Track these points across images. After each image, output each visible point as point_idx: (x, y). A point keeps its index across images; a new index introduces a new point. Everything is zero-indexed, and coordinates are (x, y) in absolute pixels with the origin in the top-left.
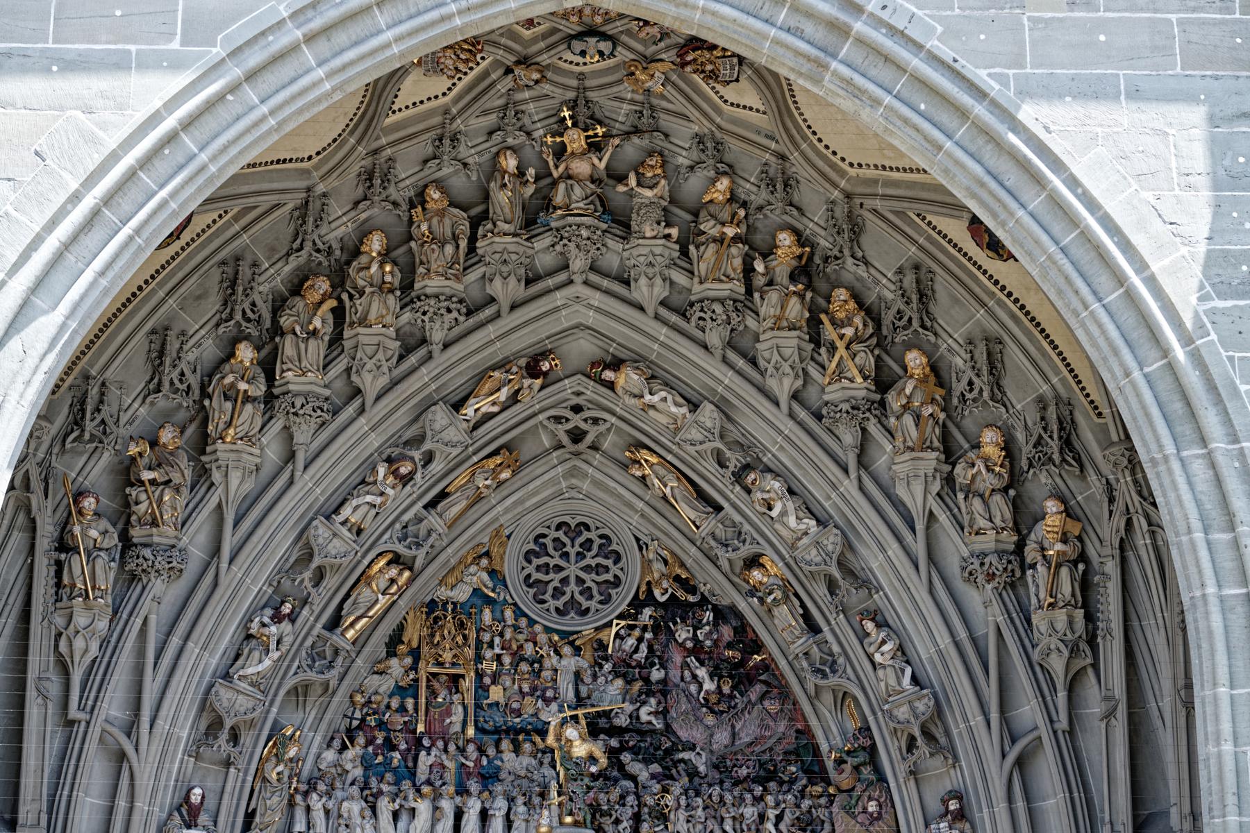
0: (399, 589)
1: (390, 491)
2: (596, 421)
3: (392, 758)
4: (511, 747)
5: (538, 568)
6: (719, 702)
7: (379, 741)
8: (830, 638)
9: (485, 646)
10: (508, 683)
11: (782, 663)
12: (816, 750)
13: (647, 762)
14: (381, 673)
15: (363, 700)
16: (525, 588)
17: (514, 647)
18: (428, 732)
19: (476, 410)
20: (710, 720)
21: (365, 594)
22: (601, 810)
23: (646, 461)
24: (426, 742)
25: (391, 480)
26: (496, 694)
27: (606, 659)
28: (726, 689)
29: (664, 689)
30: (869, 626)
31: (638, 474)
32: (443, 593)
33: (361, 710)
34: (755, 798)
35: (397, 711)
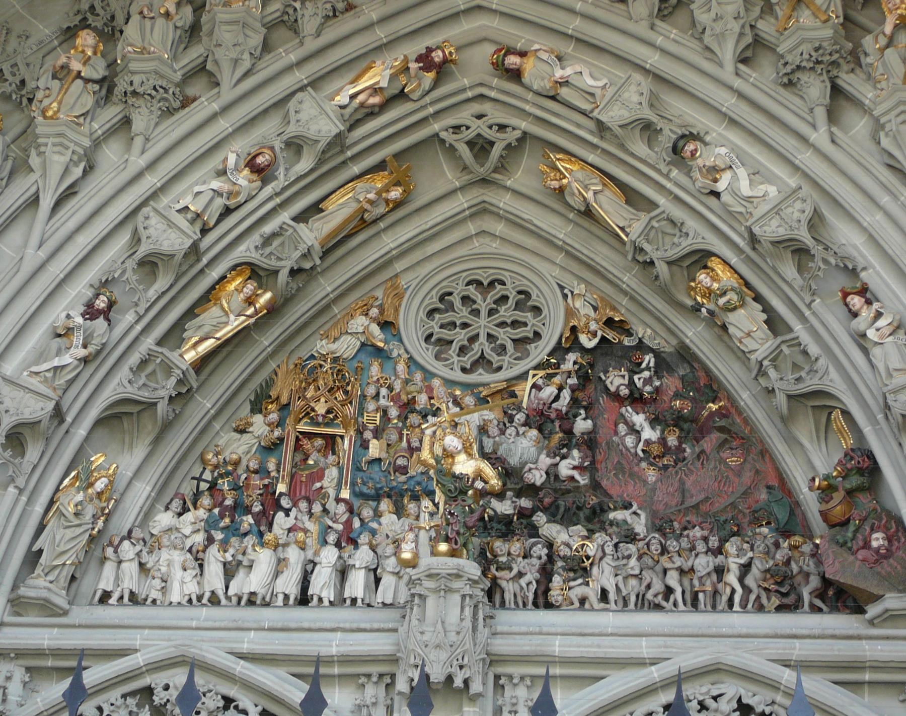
0: (257, 312)
1: (242, 182)
2: (502, 127)
3: (242, 521)
4: (392, 508)
5: (442, 326)
6: (661, 457)
7: (229, 502)
8: (805, 338)
9: (369, 399)
10: (394, 437)
11: (746, 398)
12: (795, 507)
13: (567, 519)
14: (242, 431)
15: (214, 461)
16: (424, 344)
17: (404, 398)
18: (291, 493)
19: (353, 97)
20: (652, 475)
21: (212, 314)
22: (497, 562)
23: (566, 169)
24: (285, 503)
25: (246, 172)
26: (375, 449)
27: (519, 409)
28: (672, 441)
29: (590, 443)
30: (856, 301)
31: (555, 184)
32: (323, 346)
33: (212, 472)
34: (709, 550)
35: (256, 472)
